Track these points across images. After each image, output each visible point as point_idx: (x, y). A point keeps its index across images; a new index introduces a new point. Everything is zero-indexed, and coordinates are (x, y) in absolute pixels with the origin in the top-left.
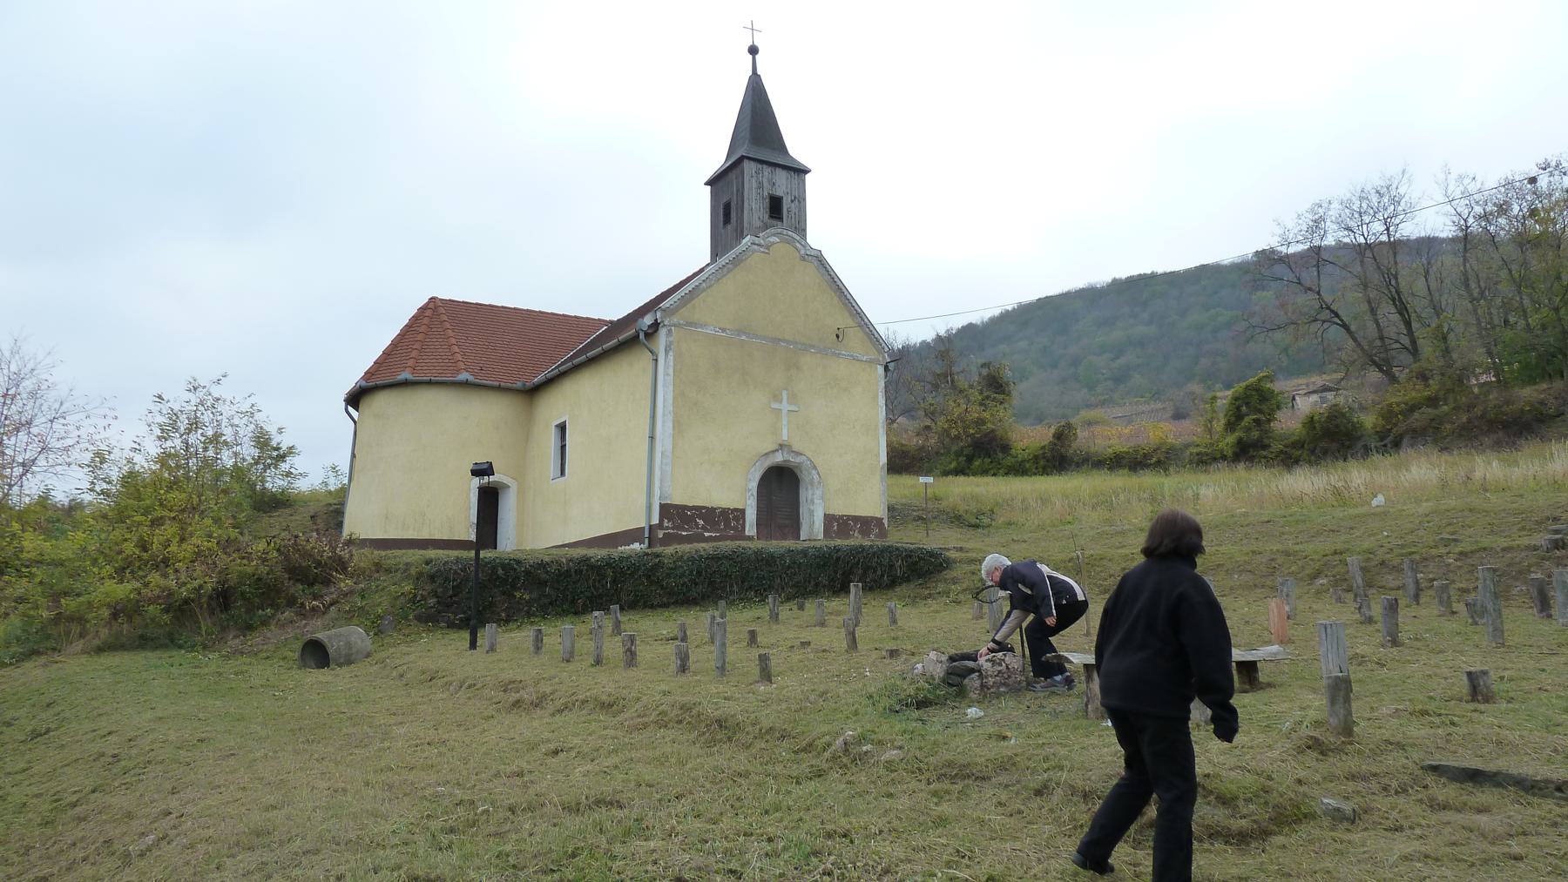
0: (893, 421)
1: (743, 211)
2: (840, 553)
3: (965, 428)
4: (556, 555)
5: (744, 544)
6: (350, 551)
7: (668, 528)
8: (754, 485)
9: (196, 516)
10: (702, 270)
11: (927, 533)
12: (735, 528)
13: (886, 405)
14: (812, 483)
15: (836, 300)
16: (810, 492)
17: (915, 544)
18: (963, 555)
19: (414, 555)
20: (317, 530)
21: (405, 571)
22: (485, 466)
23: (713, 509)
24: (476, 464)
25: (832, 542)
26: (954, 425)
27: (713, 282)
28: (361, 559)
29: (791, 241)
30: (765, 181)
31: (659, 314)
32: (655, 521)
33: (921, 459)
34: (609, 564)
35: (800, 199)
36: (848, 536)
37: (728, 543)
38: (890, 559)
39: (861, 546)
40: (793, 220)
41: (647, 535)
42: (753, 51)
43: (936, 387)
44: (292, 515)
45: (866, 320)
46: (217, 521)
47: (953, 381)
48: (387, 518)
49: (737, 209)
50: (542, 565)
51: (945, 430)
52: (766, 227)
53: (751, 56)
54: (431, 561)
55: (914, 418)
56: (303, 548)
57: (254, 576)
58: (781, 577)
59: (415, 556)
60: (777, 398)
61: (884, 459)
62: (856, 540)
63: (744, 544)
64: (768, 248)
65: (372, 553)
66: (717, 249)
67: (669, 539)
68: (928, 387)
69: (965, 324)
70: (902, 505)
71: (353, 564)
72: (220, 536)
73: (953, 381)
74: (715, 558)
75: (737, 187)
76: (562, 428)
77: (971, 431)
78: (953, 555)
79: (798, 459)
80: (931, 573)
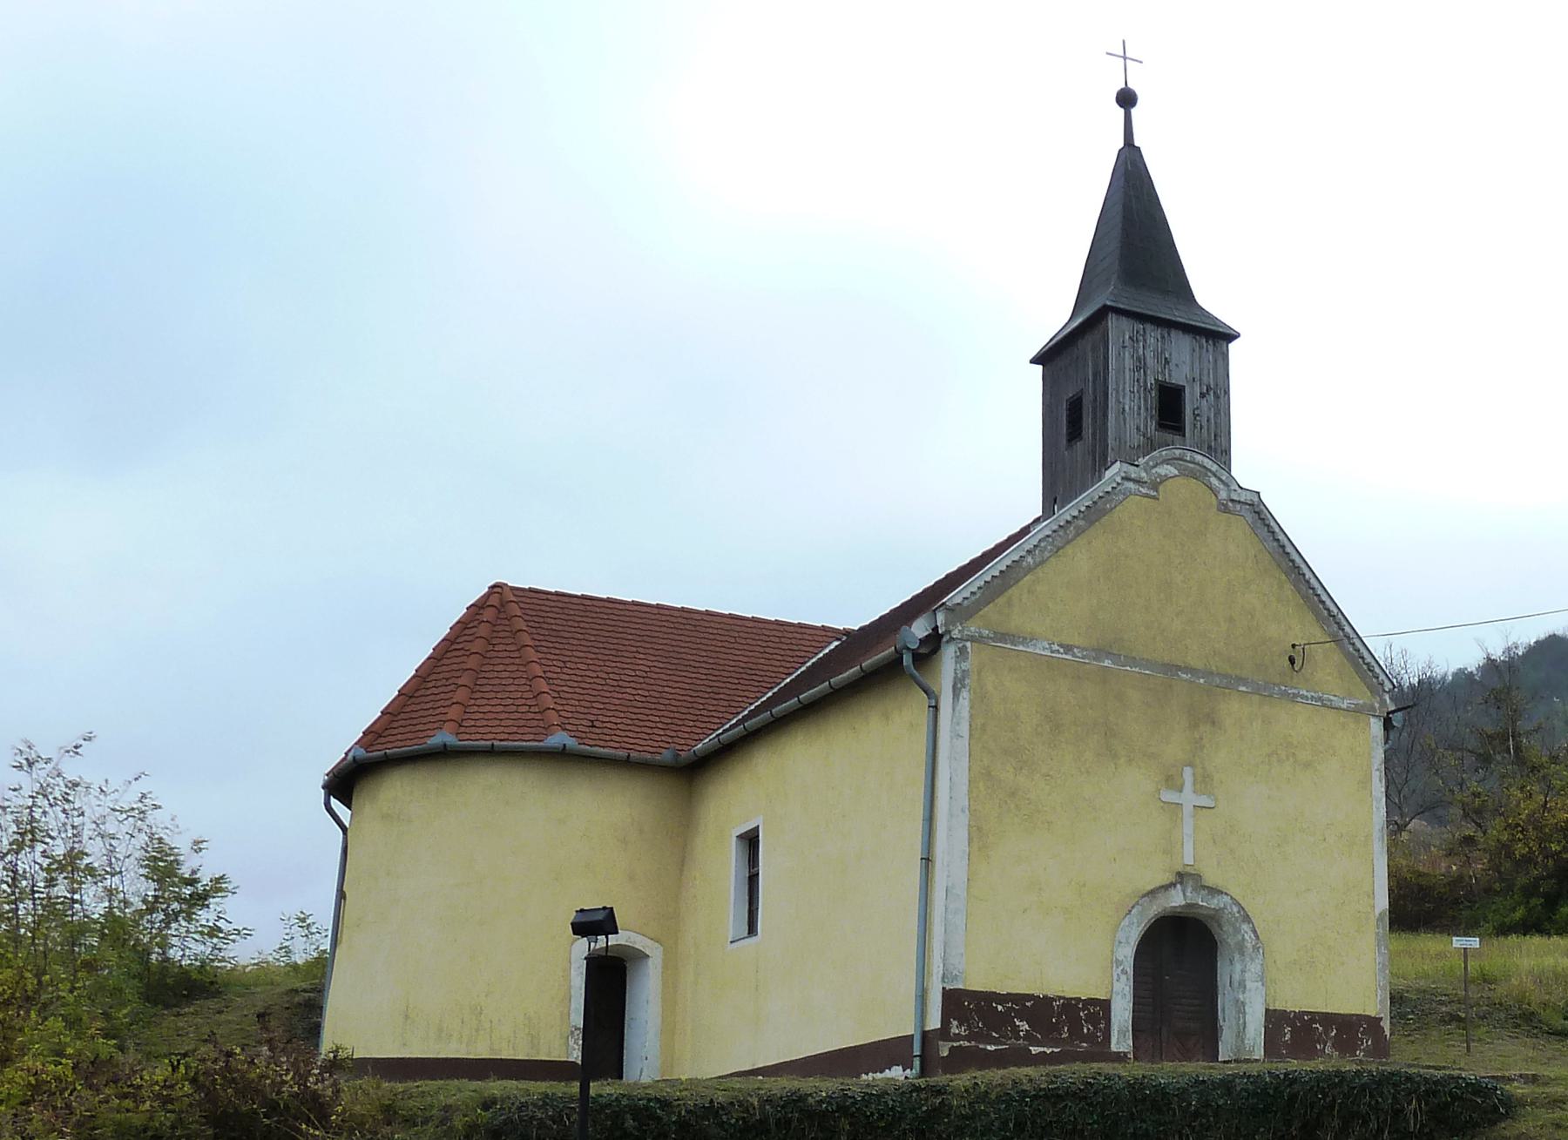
0: (1401, 828)
1: (1105, 415)
2: (1296, 1087)
3: (1543, 840)
4: (740, 1090)
5: (1107, 1068)
6: (335, 1084)
7: (958, 1037)
8: (1127, 953)
9: (33, 1015)
10: (1025, 531)
11: (1468, 1048)
12: (1090, 1038)
13: (1387, 796)
14: (1241, 948)
15: (1288, 589)
16: (1238, 967)
17: (1444, 1068)
18: (1539, 1090)
19: (459, 1090)
20: (270, 1041)
21: (442, 1123)
22: (600, 916)
23: (1047, 1001)
24: (582, 911)
25: (1280, 1065)
26: (1520, 836)
27: (1047, 554)
28: (355, 1097)
29: (1200, 474)
30: (1150, 355)
31: (940, 618)
32: (934, 1022)
33: (1456, 902)
34: (842, 1109)
35: (1219, 392)
36: (1311, 1053)
37: (1077, 1066)
38: (1394, 1097)
39: (1338, 1073)
40: (1205, 431)
41: (917, 1051)
42: (1126, 99)
43: (1485, 760)
44: (220, 1012)
45: (1347, 629)
46: (73, 1023)
47: (1518, 748)
48: (407, 1017)
49: (1094, 409)
50: (711, 1110)
51: (1504, 846)
52: (1151, 446)
53: (1122, 110)
54: (494, 1102)
55: (1441, 821)
56: (243, 1077)
57: (145, 1131)
58: (1180, 1133)
59: (463, 1091)
60: (1172, 781)
61: (1382, 902)
62: (1328, 1061)
63: (1107, 1068)
64: (1155, 487)
65: (378, 1087)
66: (1057, 487)
67: (959, 1061)
68: (1470, 760)
69: (1542, 636)
70: (1418, 991)
71: (340, 1109)
72: (79, 1053)
73: (1518, 748)
74: (1053, 1096)
75: (1095, 366)
76: (751, 841)
77: (1554, 847)
78: (1519, 1090)
79: (1215, 903)
80: (1476, 1125)
